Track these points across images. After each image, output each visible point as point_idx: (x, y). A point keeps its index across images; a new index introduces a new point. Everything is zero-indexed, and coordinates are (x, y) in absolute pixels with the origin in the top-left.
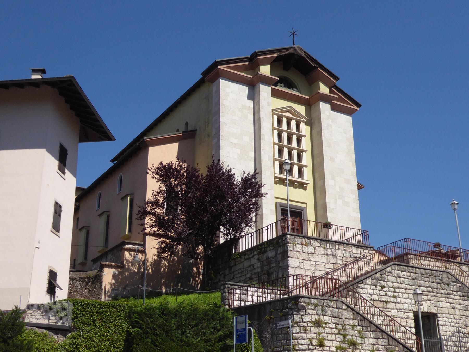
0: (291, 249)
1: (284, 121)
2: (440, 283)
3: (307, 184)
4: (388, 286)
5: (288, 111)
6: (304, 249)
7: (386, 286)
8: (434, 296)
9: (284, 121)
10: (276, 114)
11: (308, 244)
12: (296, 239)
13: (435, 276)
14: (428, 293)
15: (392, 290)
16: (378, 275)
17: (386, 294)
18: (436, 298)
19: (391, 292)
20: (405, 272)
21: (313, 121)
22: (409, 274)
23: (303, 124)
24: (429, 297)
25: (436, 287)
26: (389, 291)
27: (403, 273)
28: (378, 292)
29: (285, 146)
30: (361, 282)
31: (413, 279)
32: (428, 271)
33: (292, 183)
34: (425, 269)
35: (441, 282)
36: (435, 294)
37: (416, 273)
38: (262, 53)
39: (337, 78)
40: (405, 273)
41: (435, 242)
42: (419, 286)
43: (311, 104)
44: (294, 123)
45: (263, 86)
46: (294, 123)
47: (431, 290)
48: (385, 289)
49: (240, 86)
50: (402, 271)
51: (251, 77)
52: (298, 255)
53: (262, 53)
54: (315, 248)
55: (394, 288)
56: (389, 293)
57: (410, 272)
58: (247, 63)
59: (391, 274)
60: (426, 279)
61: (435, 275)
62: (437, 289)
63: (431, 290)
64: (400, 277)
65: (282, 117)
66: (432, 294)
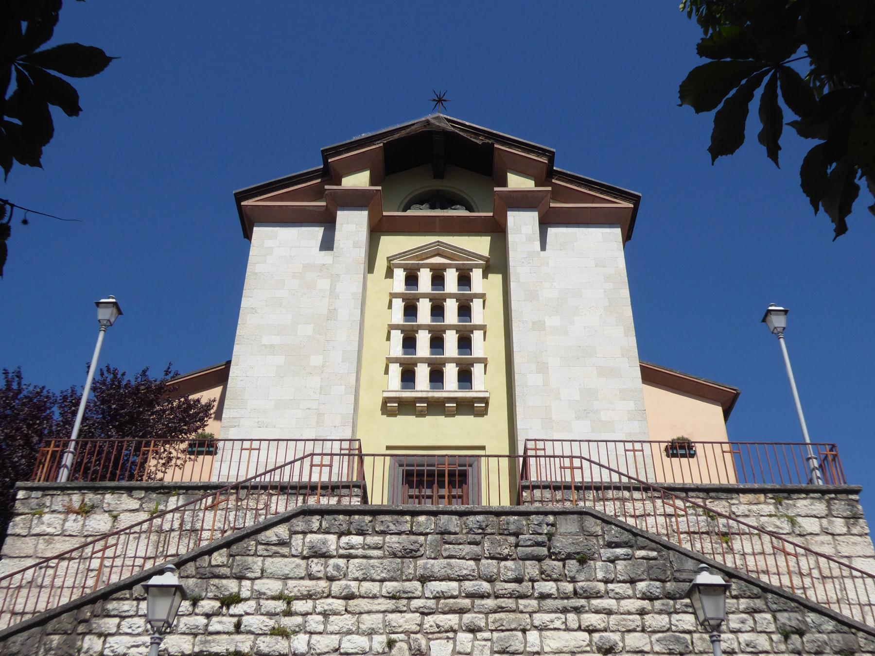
0: (18, 531)
1: (425, 277)
2: (539, 559)
3: (485, 401)
4: (259, 596)
5: (439, 254)
6: (73, 524)
7: (245, 593)
8: (500, 609)
9: (425, 277)
10: (399, 266)
11: (93, 507)
12: (47, 501)
13: (516, 534)
14: (467, 602)
15: (280, 606)
16: (218, 558)
17: (238, 626)
18: (512, 616)
19: (270, 615)
20: (361, 533)
22: (377, 539)
23: (476, 275)
24: (467, 618)
25: (511, 575)
26: (258, 611)
27: (344, 539)
28: (202, 620)
29: (421, 327)
30: (126, 593)
31: (394, 555)
32: (480, 518)
33: (436, 407)
34: (461, 514)
35: (544, 551)
36: (509, 603)
37: (412, 533)
38: (337, 151)
39: (551, 156)
40: (356, 540)
41: (671, 436)
42: (424, 580)
43: (497, 230)
44: (451, 278)
45: (346, 212)
46: (451, 278)
47: (486, 586)
48: (236, 609)
49: (304, 229)
50: (341, 534)
51: (324, 204)
52: (41, 546)
53: (337, 151)
54: (115, 518)
55: (289, 601)
56: (253, 622)
57: (383, 533)
58: (319, 180)
59: (284, 550)
60: (467, 549)
61: (512, 528)
62: (519, 580)
63: (486, 586)
64: (326, 556)
65: (418, 268)
66: (490, 603)
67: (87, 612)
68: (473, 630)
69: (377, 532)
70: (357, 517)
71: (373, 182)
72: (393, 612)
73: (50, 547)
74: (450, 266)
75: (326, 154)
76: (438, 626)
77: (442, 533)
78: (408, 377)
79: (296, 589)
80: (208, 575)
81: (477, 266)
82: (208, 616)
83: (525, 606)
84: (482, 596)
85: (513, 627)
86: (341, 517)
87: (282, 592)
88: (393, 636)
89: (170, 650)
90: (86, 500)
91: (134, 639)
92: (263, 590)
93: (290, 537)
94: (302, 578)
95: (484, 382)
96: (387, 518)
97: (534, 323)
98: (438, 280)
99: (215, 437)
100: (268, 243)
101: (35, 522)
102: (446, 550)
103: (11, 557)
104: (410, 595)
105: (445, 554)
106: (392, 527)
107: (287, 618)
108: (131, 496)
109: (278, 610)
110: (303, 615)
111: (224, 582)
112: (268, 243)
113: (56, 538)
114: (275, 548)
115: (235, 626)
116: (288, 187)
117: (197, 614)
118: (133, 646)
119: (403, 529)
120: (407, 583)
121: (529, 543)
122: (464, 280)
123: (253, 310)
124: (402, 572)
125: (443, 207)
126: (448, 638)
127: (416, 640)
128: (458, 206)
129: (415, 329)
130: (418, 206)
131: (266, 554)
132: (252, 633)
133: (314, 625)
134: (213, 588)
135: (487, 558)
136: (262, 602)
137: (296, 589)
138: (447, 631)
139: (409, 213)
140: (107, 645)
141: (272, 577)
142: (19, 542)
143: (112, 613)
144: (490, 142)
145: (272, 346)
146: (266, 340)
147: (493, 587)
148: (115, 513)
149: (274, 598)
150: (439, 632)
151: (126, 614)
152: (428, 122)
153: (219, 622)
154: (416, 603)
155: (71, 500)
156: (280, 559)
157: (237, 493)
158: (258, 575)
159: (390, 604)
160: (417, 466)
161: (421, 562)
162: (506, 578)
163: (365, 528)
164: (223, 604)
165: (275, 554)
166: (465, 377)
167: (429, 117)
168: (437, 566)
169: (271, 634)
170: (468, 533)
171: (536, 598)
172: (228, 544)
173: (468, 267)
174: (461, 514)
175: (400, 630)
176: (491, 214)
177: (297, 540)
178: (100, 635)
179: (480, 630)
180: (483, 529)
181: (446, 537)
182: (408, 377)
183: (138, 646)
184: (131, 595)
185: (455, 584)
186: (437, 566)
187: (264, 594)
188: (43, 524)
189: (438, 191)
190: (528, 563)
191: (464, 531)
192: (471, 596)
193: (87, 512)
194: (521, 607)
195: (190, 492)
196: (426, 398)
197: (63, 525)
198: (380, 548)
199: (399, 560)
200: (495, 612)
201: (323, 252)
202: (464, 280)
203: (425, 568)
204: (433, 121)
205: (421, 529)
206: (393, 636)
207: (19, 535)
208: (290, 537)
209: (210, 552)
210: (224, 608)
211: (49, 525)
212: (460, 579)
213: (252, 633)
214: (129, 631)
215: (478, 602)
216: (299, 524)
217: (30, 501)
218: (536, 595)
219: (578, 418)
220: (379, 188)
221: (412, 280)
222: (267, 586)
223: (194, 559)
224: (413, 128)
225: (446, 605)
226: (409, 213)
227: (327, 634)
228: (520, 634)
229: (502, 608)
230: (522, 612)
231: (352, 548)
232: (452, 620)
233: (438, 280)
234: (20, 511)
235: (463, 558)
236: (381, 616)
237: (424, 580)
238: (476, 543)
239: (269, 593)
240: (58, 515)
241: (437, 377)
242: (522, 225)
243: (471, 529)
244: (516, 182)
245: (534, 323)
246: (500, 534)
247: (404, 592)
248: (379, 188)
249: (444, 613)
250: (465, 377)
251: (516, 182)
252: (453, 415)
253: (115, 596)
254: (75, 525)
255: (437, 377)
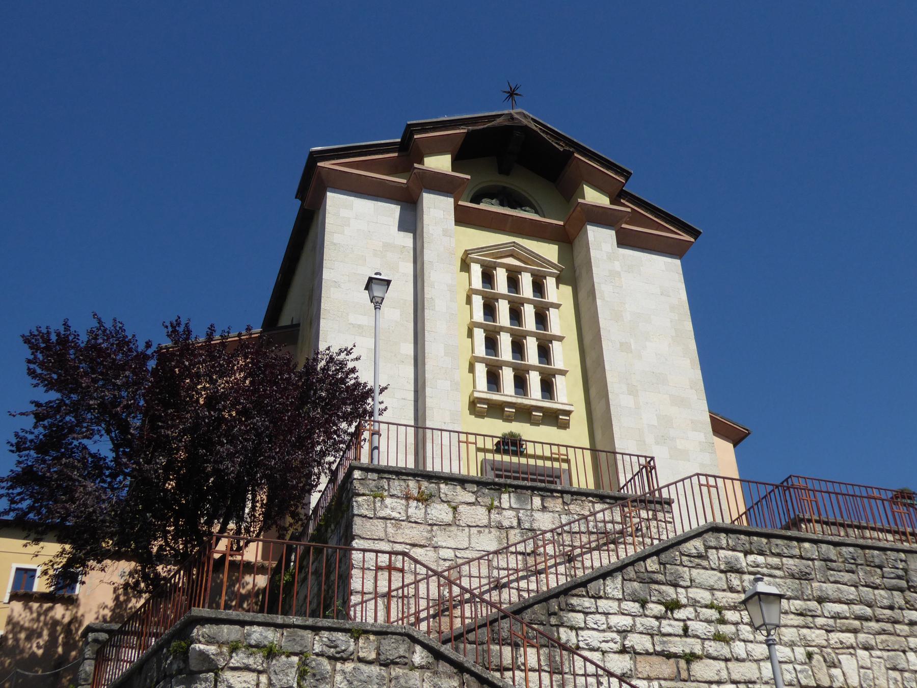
0: (364, 512)
1: (501, 276)
2: (901, 590)
3: (568, 413)
4: (694, 603)
5: (512, 255)
6: (416, 510)
7: (684, 601)
8: (883, 632)
9: (501, 276)
10: (476, 261)
11: (431, 496)
12: (384, 483)
13: (880, 567)
14: (857, 623)
15: (713, 614)
16: (652, 564)
17: (686, 629)
18: (892, 638)
19: (709, 622)
20: (761, 553)
21: (575, 273)
22: (775, 561)
23: (550, 282)
24: (862, 637)
25: (886, 602)
26: (697, 618)
27: (751, 558)
28: (655, 623)
29: (502, 329)
30: (582, 591)
31: (793, 576)
32: (851, 549)
33: (525, 414)
34: (836, 544)
35: (903, 584)
36: (888, 627)
37: (801, 557)
38: (424, 128)
39: (627, 175)
40: (760, 559)
41: (898, 486)
42: (821, 600)
43: (568, 239)
44: (526, 281)
45: (432, 196)
46: (526, 281)
47: (868, 611)
48: (680, 614)
49: (380, 204)
50: (746, 553)
51: (405, 181)
52: (391, 530)
53: (424, 128)
54: (455, 509)
55: (720, 609)
56: (696, 627)
57: (779, 555)
58: (396, 154)
59: (705, 563)
60: (847, 577)
61: (877, 561)
62: (891, 608)
63: (868, 611)
64: (739, 571)
65: (494, 266)
66: (873, 625)
67: (554, 605)
68: (867, 648)
69: (773, 554)
70: (755, 538)
71: (455, 166)
72: (803, 627)
73: (400, 531)
74: (526, 270)
75: (410, 131)
76: (841, 643)
77: (825, 560)
78: (494, 380)
79: (724, 600)
80: (647, 580)
81: (551, 275)
82: (657, 618)
83: (901, 631)
84: (867, 619)
85: (896, 647)
86: (742, 536)
87: (712, 603)
88: (810, 649)
89: (636, 647)
90: (423, 488)
91: (602, 635)
92: (698, 599)
93: (706, 551)
94: (724, 590)
95: (569, 393)
96: (779, 542)
97: (621, 344)
98: (513, 283)
99: (523, 438)
100: (344, 213)
101: (378, 504)
102: (831, 575)
103: (363, 538)
104: (814, 613)
105: (832, 579)
106: (785, 551)
107: (722, 626)
108: (465, 489)
109: (714, 618)
110: (734, 624)
111: (664, 588)
112: (344, 213)
113: (403, 523)
114: (697, 560)
115: (684, 630)
116: (366, 155)
117: (646, 616)
118: (604, 641)
119: (794, 553)
120: (808, 603)
121: (892, 576)
122: (539, 288)
123: (337, 284)
124: (802, 593)
125: (513, 207)
126: (851, 654)
127: (829, 654)
128: (528, 209)
129: (497, 330)
130: (489, 200)
131: (691, 565)
132: (698, 637)
133: (747, 634)
134: (656, 593)
135: (863, 586)
136: (699, 609)
137: (724, 600)
138: (848, 648)
139: (483, 206)
140: (580, 638)
141: (700, 587)
142: (368, 524)
143: (577, 608)
144: (571, 150)
145: (360, 326)
146: (352, 319)
147: (874, 611)
148: (453, 504)
149: (706, 606)
150: (843, 648)
151: (589, 610)
152: (511, 117)
153: (670, 625)
154: (820, 621)
155: (408, 486)
156: (703, 571)
157: (562, 497)
158: (689, 584)
159: (799, 620)
160: (506, 471)
161: (815, 584)
162: (882, 605)
163: (764, 549)
164: (667, 608)
165: (698, 566)
166: (548, 388)
167: (512, 112)
168: (830, 589)
169: (714, 640)
170: (843, 562)
171: (907, 624)
172: (657, 553)
173: (542, 274)
174: (836, 544)
175: (814, 644)
176: (562, 223)
177: (712, 554)
178: (572, 628)
179: (872, 649)
180: (855, 560)
181: (829, 564)
182: (494, 380)
183: (607, 642)
184: (587, 592)
185: (845, 607)
186: (830, 589)
187: (699, 602)
188: (386, 507)
189: (504, 188)
190: (895, 593)
191: (840, 560)
192: (858, 618)
193: (427, 500)
194: (898, 631)
195: (519, 491)
196: (515, 404)
197: (407, 511)
198: (779, 569)
199: (797, 581)
200: (880, 634)
201: (402, 233)
202: (539, 288)
203: (821, 590)
204: (516, 116)
205: (809, 555)
206: (810, 649)
207: (365, 516)
208: (706, 551)
209: (644, 558)
210: (669, 612)
211: (393, 509)
212: (849, 602)
213: (698, 637)
214: (595, 626)
215: (865, 624)
216: (711, 539)
217: (368, 482)
218: (906, 621)
219: (657, 443)
220: (469, 177)
221: (488, 278)
222: (700, 595)
223: (632, 563)
224: (499, 120)
225: (844, 624)
226: (483, 206)
227: (757, 642)
228: (901, 654)
229: (884, 630)
230: (899, 635)
231: (758, 566)
232: (849, 638)
233: (513, 283)
234: (361, 492)
235: (846, 584)
236: (795, 630)
237: (821, 600)
238: (853, 572)
239: (703, 602)
240: (399, 500)
241: (521, 383)
242: (600, 241)
243: (846, 559)
244: (593, 197)
245: (621, 344)
246: (868, 565)
247: (810, 611)
248: (469, 177)
249: (842, 631)
250: (548, 388)
251: (593, 197)
252: (538, 424)
253: (574, 592)
254: (417, 511)
255: (521, 383)
